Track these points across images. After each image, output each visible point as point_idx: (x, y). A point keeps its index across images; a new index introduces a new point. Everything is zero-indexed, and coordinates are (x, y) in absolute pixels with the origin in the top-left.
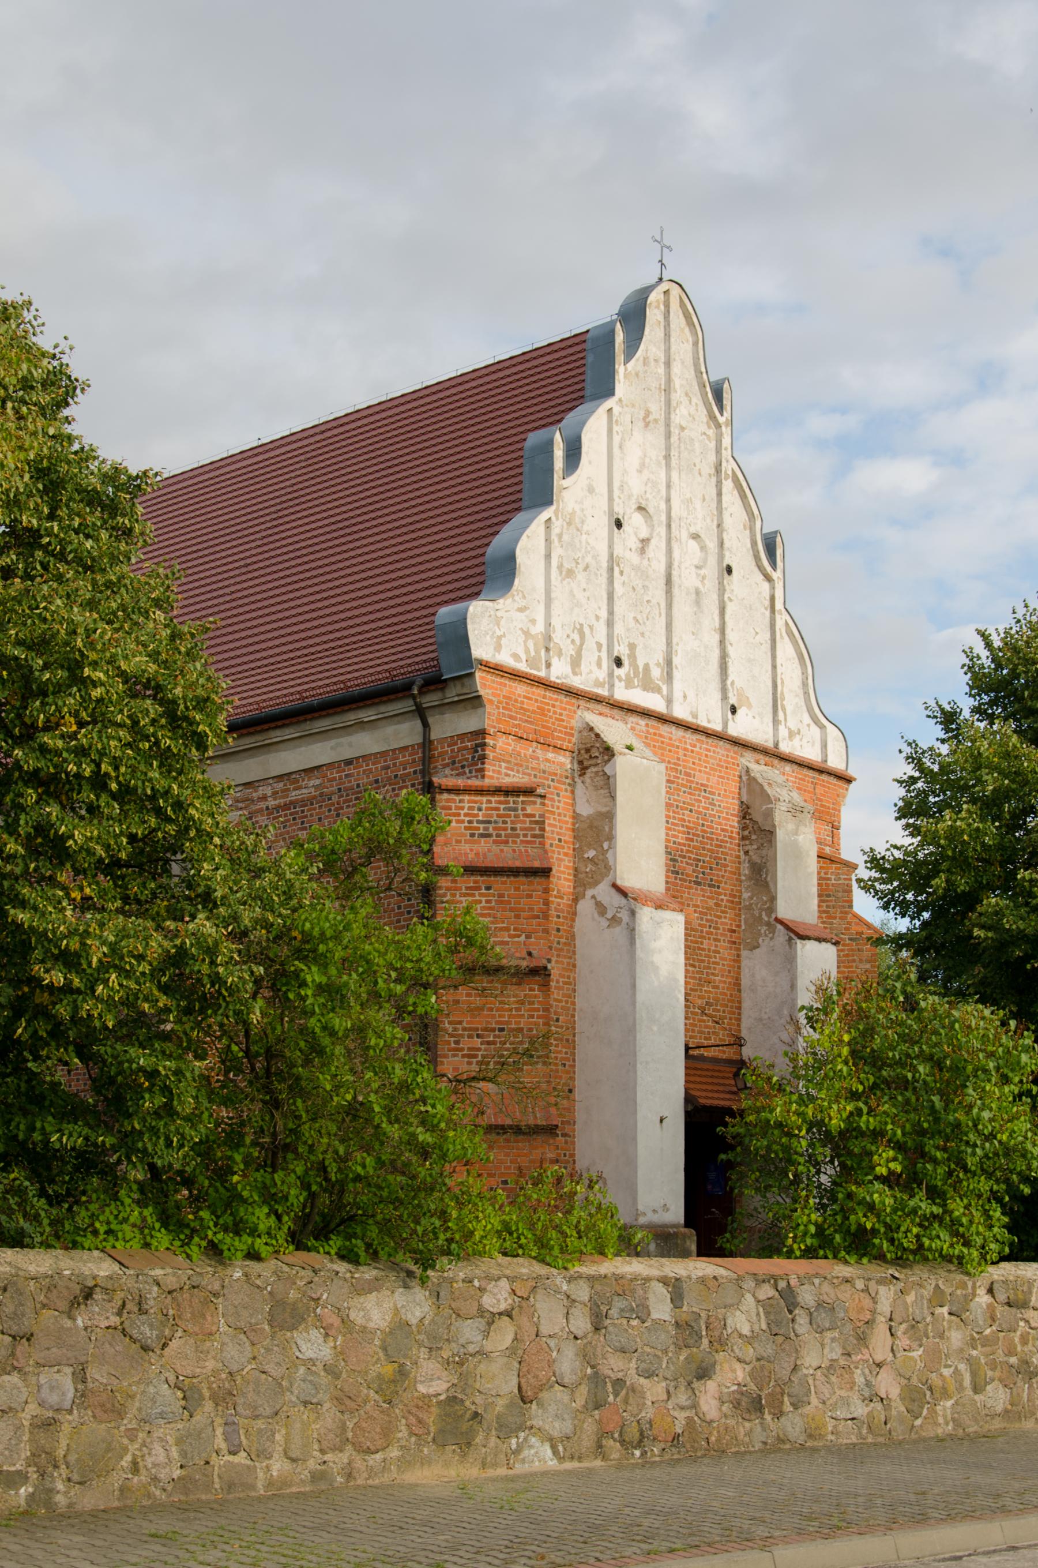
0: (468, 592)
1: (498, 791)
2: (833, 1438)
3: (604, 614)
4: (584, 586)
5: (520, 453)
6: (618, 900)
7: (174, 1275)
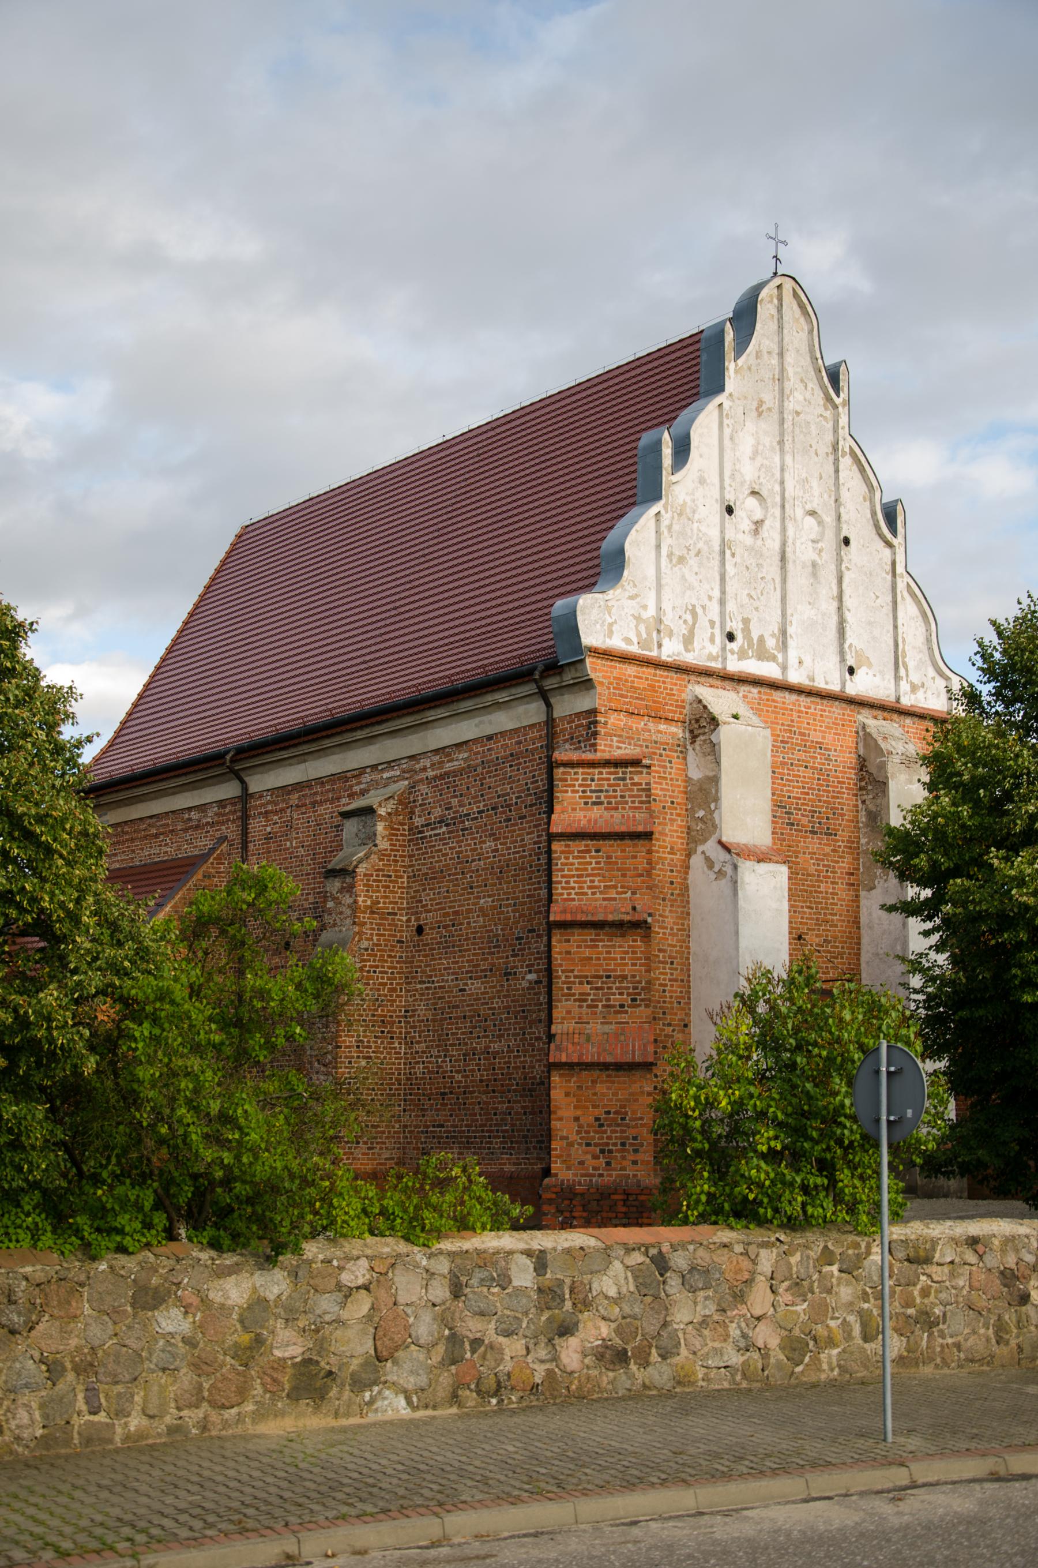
0: (586, 582)
1: (607, 763)
2: (704, 1384)
3: (716, 593)
4: (696, 569)
5: (634, 452)
6: (723, 855)
7: (43, 1270)
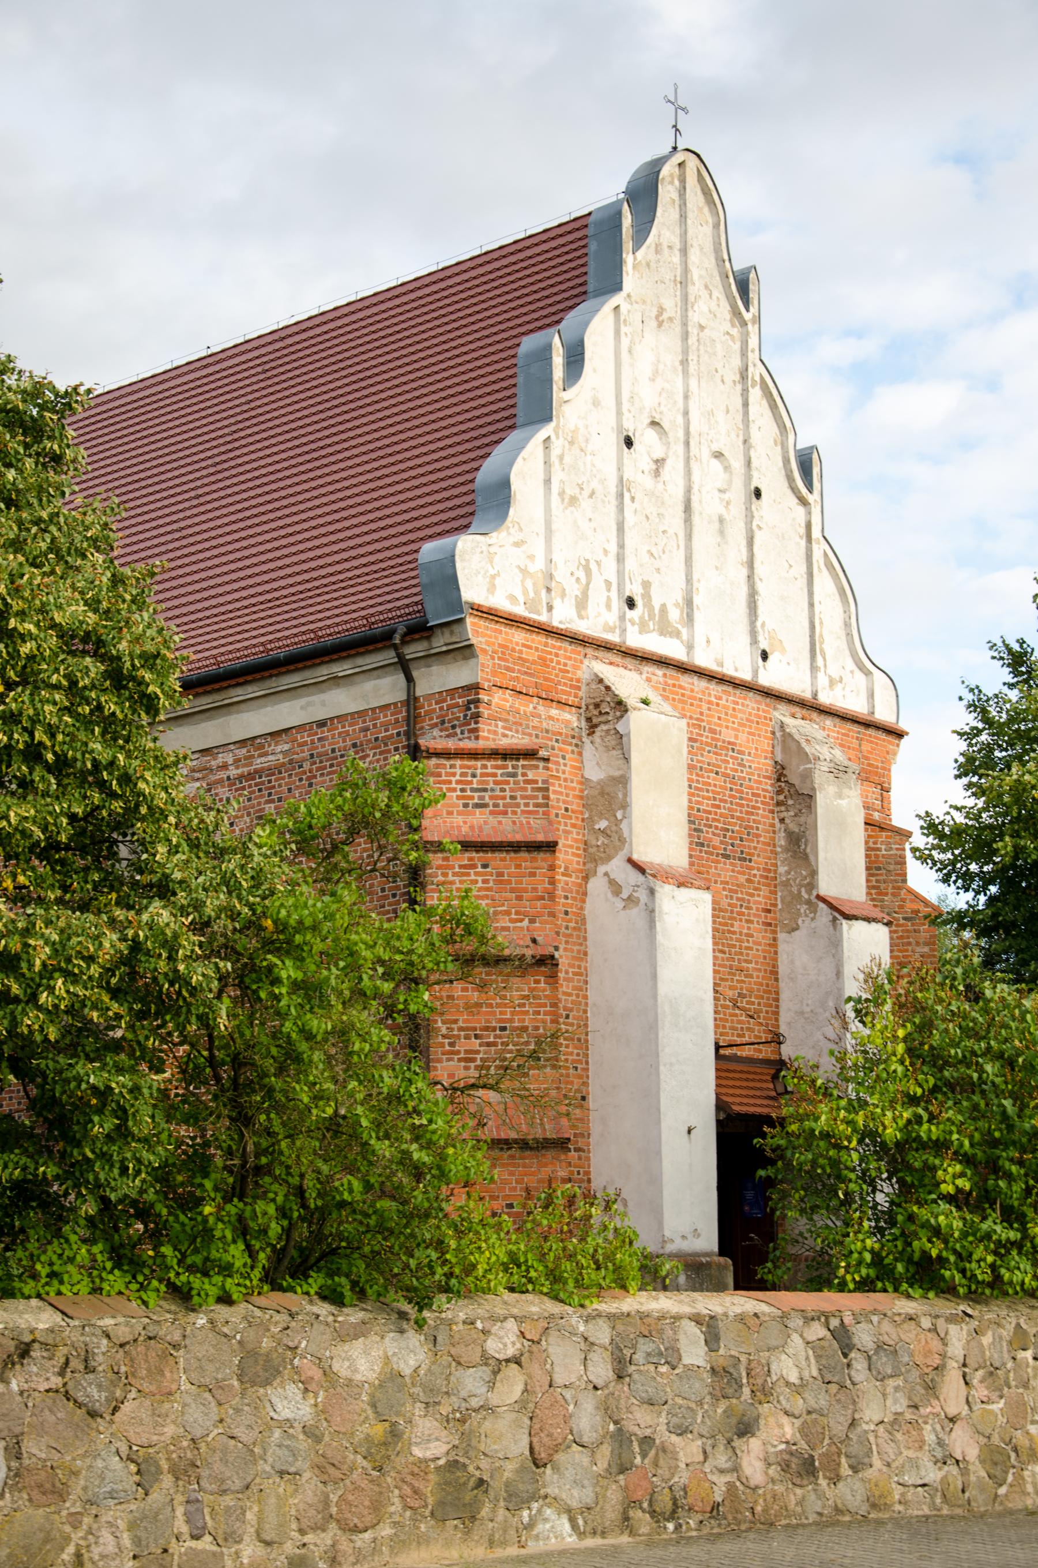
0: (456, 524)
3: (613, 548)
5: (513, 361)
6: (634, 877)
7: (127, 1324)
